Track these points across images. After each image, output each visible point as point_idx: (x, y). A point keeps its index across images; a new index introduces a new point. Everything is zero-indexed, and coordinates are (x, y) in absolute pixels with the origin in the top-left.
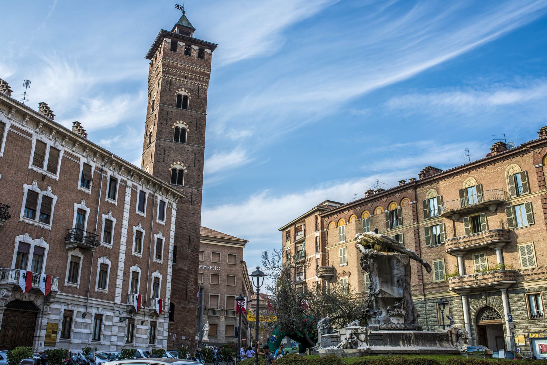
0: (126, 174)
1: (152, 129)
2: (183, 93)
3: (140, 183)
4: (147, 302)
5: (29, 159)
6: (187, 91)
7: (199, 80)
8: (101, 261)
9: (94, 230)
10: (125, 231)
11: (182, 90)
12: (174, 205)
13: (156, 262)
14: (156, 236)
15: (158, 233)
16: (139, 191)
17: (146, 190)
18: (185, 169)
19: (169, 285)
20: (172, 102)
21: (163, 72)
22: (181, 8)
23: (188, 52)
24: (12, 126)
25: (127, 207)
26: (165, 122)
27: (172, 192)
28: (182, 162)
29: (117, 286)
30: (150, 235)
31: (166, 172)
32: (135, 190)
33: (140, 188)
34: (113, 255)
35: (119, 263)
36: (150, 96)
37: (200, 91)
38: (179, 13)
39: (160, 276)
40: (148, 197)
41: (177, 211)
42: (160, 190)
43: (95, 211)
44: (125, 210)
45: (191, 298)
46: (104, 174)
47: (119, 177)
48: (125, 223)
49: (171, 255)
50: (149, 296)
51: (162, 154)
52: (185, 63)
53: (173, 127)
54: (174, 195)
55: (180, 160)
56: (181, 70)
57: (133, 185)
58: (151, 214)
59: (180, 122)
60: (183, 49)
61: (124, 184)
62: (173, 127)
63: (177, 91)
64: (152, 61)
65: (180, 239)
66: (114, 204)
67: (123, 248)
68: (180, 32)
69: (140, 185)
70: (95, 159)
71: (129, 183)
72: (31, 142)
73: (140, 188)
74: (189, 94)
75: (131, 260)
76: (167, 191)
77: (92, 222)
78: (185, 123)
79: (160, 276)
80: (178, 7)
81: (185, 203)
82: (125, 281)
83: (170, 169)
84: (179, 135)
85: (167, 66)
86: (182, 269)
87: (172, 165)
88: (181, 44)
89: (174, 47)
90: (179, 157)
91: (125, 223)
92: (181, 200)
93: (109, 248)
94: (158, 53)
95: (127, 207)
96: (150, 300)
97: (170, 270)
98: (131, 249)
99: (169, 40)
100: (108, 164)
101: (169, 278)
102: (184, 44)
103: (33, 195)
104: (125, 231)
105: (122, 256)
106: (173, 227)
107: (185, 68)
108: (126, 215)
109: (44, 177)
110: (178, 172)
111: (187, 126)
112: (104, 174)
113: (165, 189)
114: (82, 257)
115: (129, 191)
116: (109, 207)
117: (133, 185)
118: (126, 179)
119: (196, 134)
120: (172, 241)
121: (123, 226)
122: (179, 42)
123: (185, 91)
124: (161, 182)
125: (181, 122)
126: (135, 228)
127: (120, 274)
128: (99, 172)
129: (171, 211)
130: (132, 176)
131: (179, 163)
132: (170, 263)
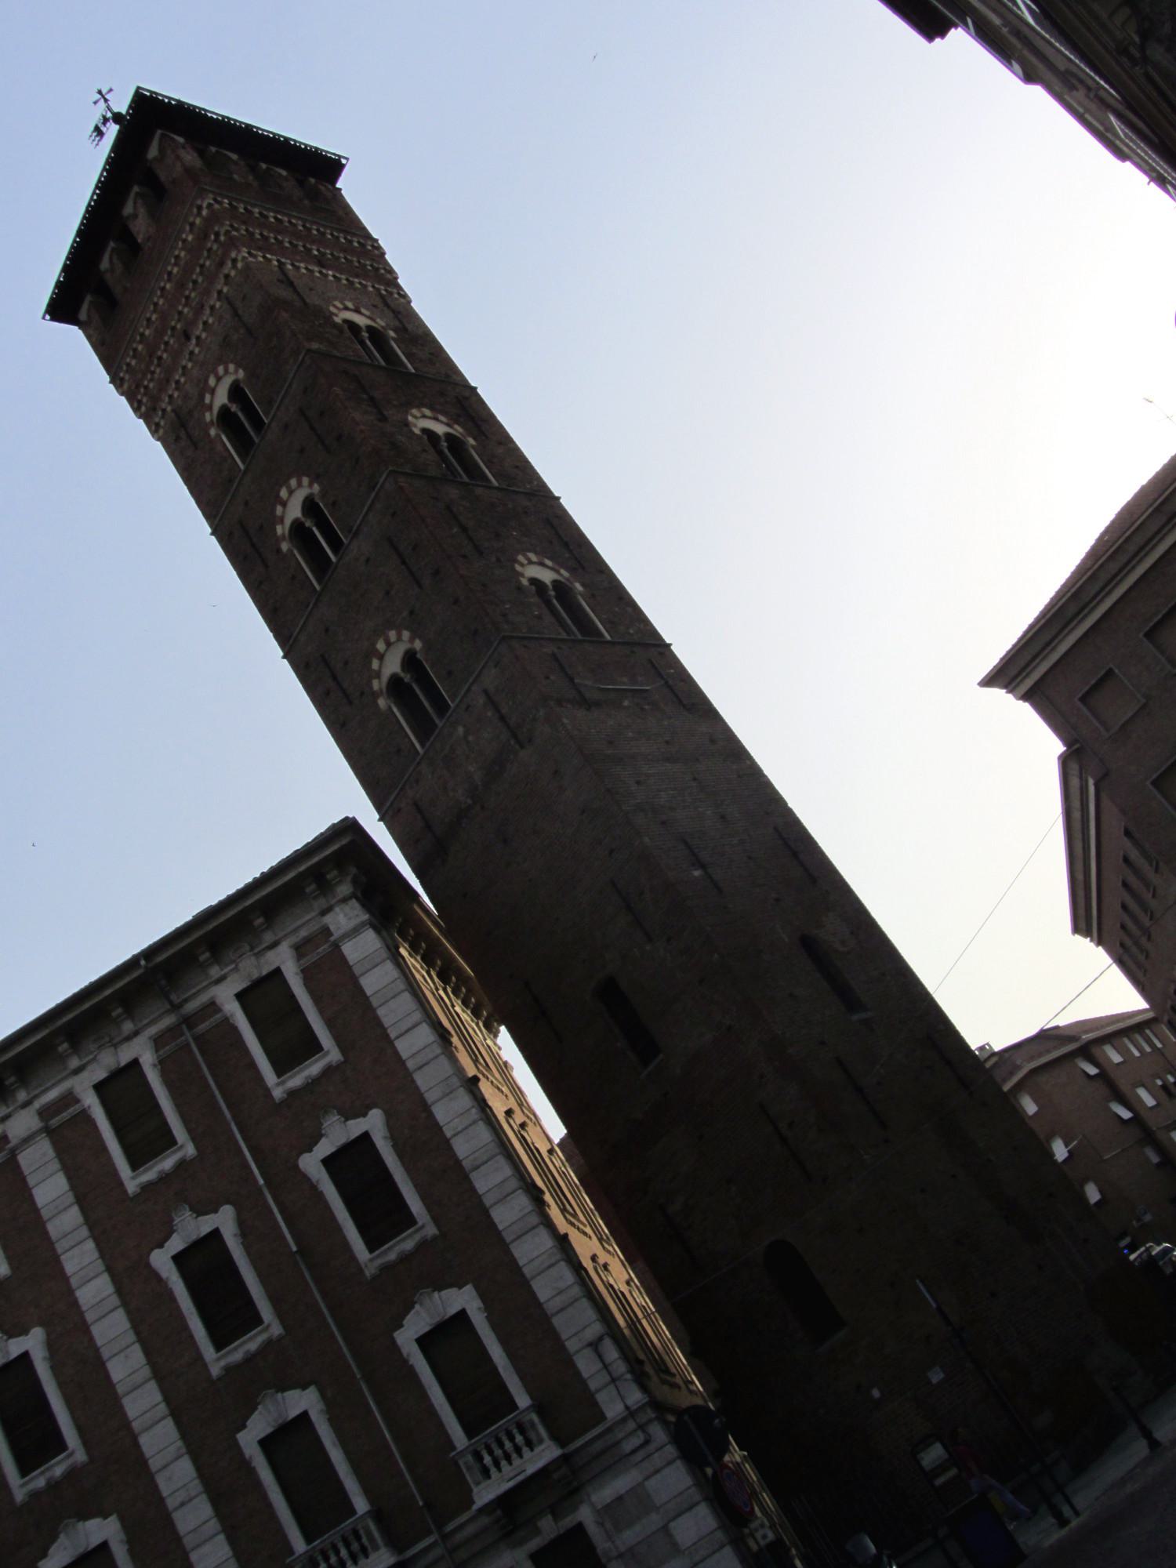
10: (111, 1328)
14: (311, 1164)
15: (316, 1137)
18: (412, 640)
48: (94, 1291)
57: (45, 1113)
67: (142, 1401)
78: (293, 482)
91: (94, 1291)
98: (199, 1357)
104: (111, 1328)
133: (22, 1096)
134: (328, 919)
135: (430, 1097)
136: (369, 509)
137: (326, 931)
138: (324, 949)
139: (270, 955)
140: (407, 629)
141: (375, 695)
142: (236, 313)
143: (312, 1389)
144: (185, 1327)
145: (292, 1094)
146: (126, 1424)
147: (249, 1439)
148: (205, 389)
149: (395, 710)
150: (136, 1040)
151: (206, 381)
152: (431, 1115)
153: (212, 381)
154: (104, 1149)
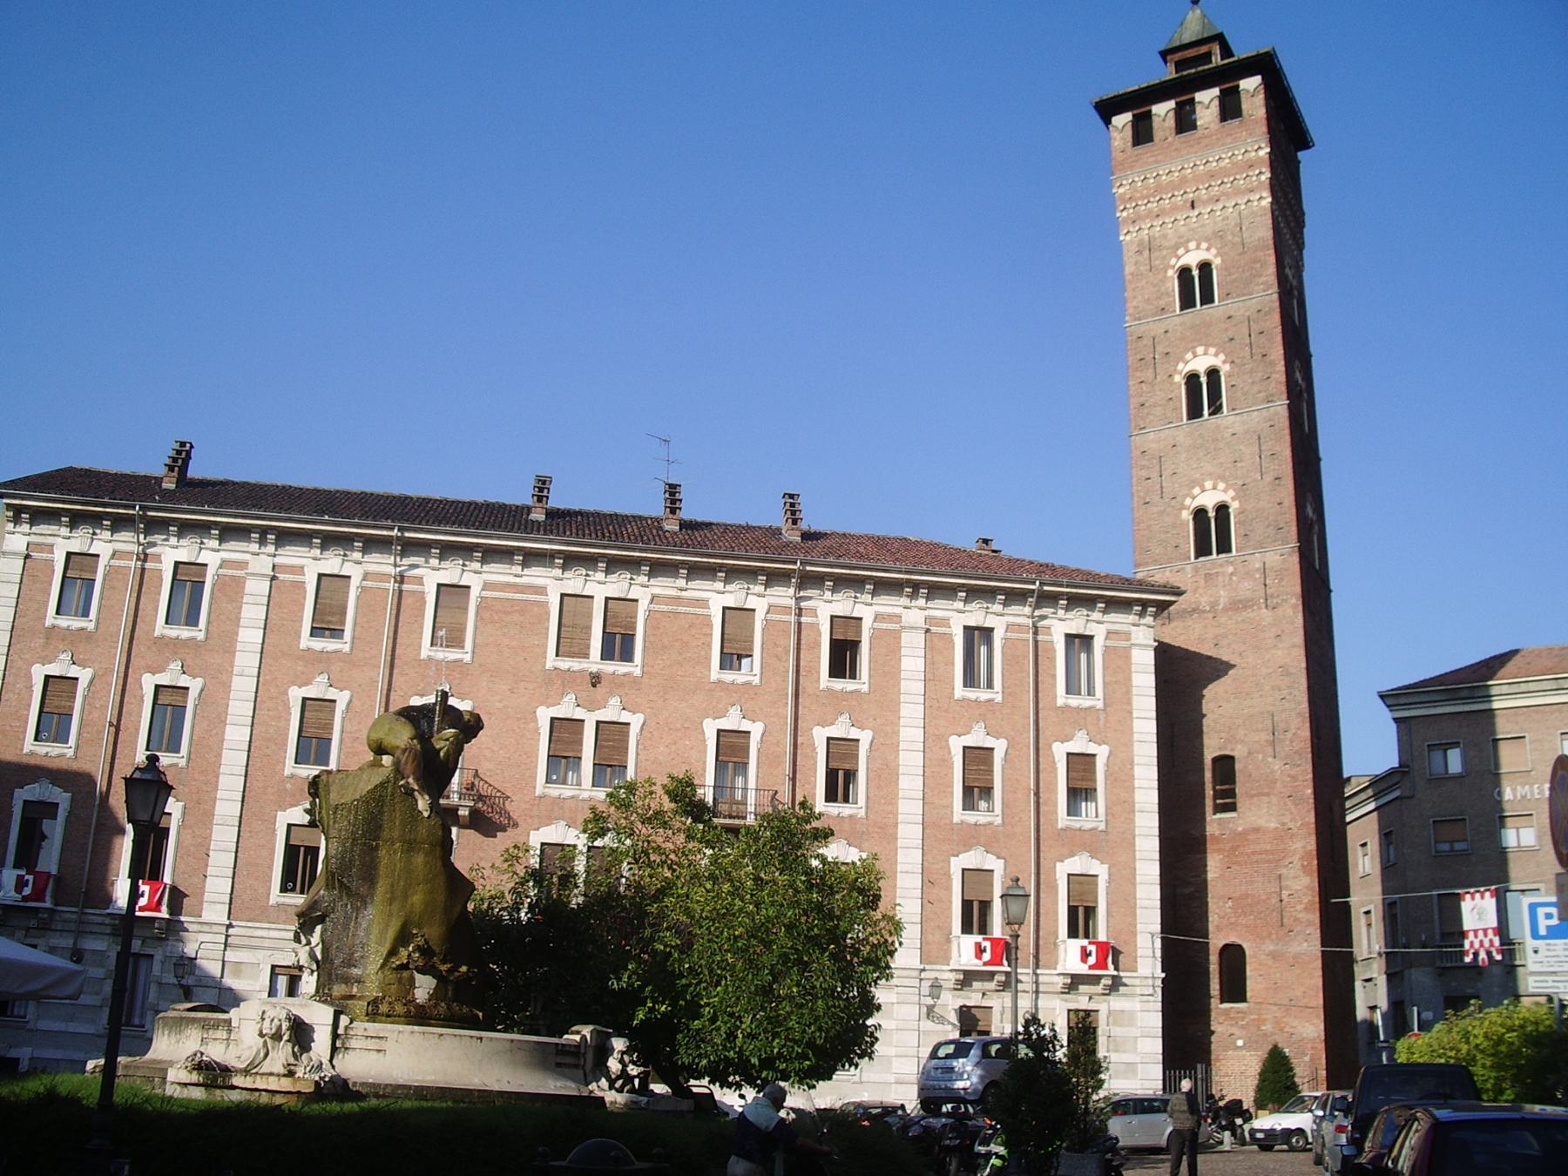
5: (545, 646)
6: (1204, 245)
10: (910, 761)
18: (1233, 499)
20: (1162, 303)
24: (487, 586)
26: (1149, 374)
31: (1174, 526)
45: (1296, 920)
48: (911, 733)
51: (1155, 475)
55: (1210, 475)
60: (1171, 122)
65: (1241, 732)
72: (544, 605)
78: (1212, 350)
81: (1245, 607)
86: (1257, 830)
91: (911, 733)
103: (564, 730)
104: (910, 761)
108: (911, 712)
109: (596, 680)
110: (1212, 514)
111: (1222, 357)
119: (1251, 371)
131: (1208, 484)
133: (921, 602)
135: (1137, 760)
137: (1127, 636)
138: (1124, 644)
141: (1183, 507)
144: (952, 786)
145: (1067, 706)
146: (896, 814)
147: (957, 864)
148: (1183, 243)
151: (1188, 241)
153: (1192, 245)
154: (953, 664)
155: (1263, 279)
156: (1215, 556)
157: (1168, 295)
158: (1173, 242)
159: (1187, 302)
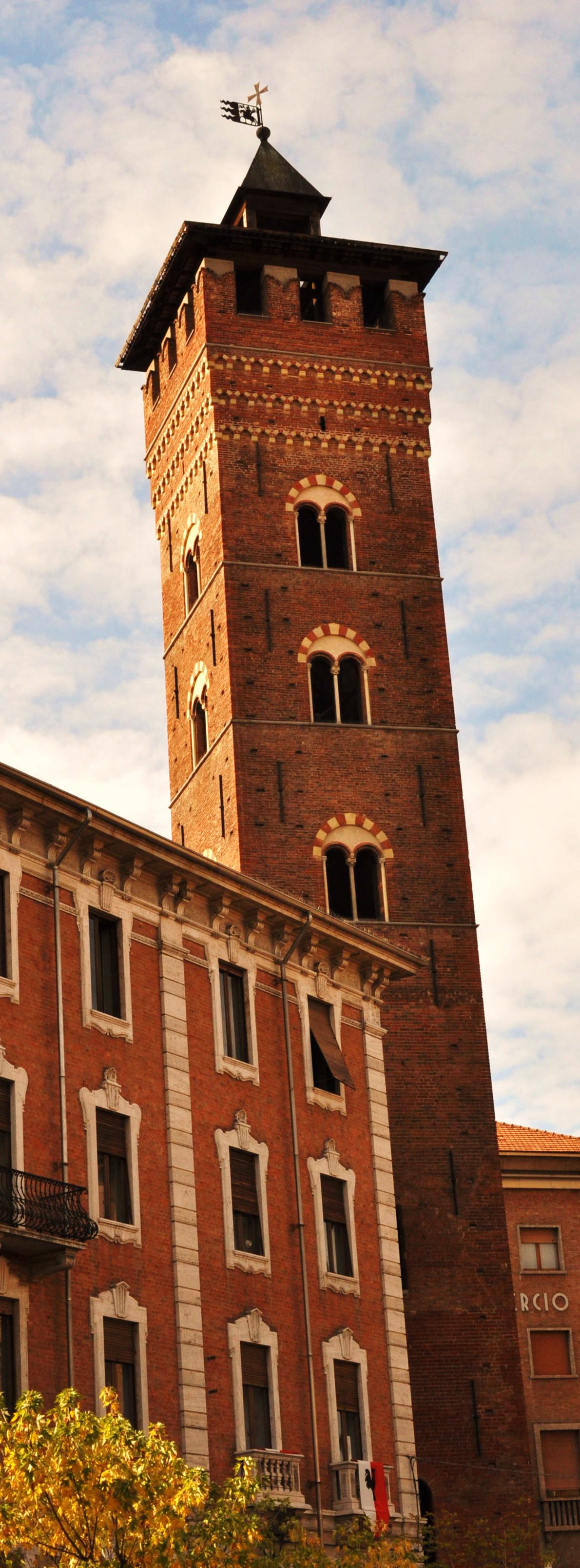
0: (152, 894)
1: (203, 680)
2: (322, 497)
3: (216, 926)
4: (323, 1485)
7: (383, 426)
8: (103, 1307)
9: (58, 1166)
10: (183, 1159)
11: (314, 484)
12: (372, 1015)
13: (331, 1290)
15: (320, 1154)
16: (214, 967)
17: (244, 960)
18: (385, 845)
19: (402, 1395)
21: (220, 414)
22: (248, 114)
23: (313, 307)
25: (177, 1043)
26: (260, 641)
27: (356, 955)
28: (364, 812)
29: (188, 1421)
30: (288, 1166)
32: (198, 960)
33: (217, 951)
34: (150, 1274)
35: (182, 1308)
36: (168, 533)
37: (396, 475)
38: (247, 133)
39: (359, 1356)
40: (257, 990)
41: (384, 1039)
42: (303, 950)
43: (46, 1082)
44: (170, 1059)
46: (61, 906)
47: (125, 911)
48: (180, 1119)
49: (391, 1252)
50: (327, 1452)
51: (271, 787)
52: (312, 360)
53: (302, 658)
54: (364, 967)
55: (353, 807)
56: (296, 392)
57: (187, 941)
58: (278, 1063)
59: (327, 633)
61: (147, 941)
62: (302, 658)
63: (293, 492)
64: (155, 376)
66: (122, 1039)
67: (186, 1238)
68: (260, 225)
69: (214, 935)
70: (16, 840)
71: (171, 933)
73: (217, 951)
74: (351, 497)
75: (228, 1295)
76: (334, 954)
77: (44, 1132)
78: (351, 633)
79: (359, 1356)
80: (235, 112)
82: (217, 1393)
83: (317, 852)
84: (334, 690)
85: (233, 384)
87: (321, 835)
88: (281, 274)
89: (250, 296)
90: (349, 794)
91: (180, 1119)
92: (395, 992)
93: (129, 1246)
94: (181, 332)
95: (177, 1043)
96: (333, 1473)
97: (396, 1323)
98: (222, 1241)
99: (224, 267)
100: (72, 858)
101: (399, 1360)
102: (293, 273)
104: (183, 1159)
105: (188, 1278)
106: (380, 1115)
107: (311, 381)
108: (178, 1082)
110: (352, 860)
111: (365, 646)
112: (61, 906)
113: (326, 941)
114: (22, 1295)
115: (173, 969)
116: (100, 1058)
117: (187, 941)
118: (152, 917)
120: (385, 1184)
121: (174, 1136)
122: (269, 270)
123: (329, 485)
124: (305, 913)
125: (334, 628)
126: (226, 1140)
127: (192, 1359)
128: (41, 898)
129: (363, 1045)
130: (178, 899)
131: (350, 818)
132: (393, 1288)
134: (364, 1004)
136: (417, 731)
139: (332, 990)
140: (387, 833)
142: (389, 473)
143: (275, 1333)
149: (325, 868)
150: (250, 955)
152: (375, 1209)
153: (321, 479)
155: (419, 557)
156: (356, 920)
157: (288, 539)
158: (293, 465)
159: (311, 556)
